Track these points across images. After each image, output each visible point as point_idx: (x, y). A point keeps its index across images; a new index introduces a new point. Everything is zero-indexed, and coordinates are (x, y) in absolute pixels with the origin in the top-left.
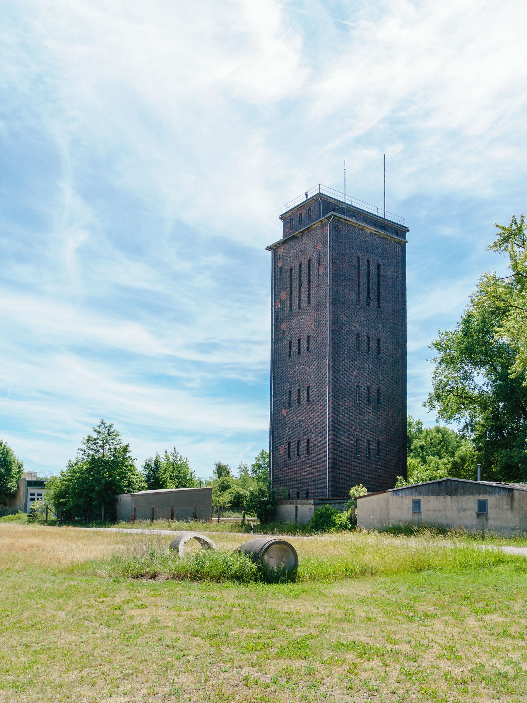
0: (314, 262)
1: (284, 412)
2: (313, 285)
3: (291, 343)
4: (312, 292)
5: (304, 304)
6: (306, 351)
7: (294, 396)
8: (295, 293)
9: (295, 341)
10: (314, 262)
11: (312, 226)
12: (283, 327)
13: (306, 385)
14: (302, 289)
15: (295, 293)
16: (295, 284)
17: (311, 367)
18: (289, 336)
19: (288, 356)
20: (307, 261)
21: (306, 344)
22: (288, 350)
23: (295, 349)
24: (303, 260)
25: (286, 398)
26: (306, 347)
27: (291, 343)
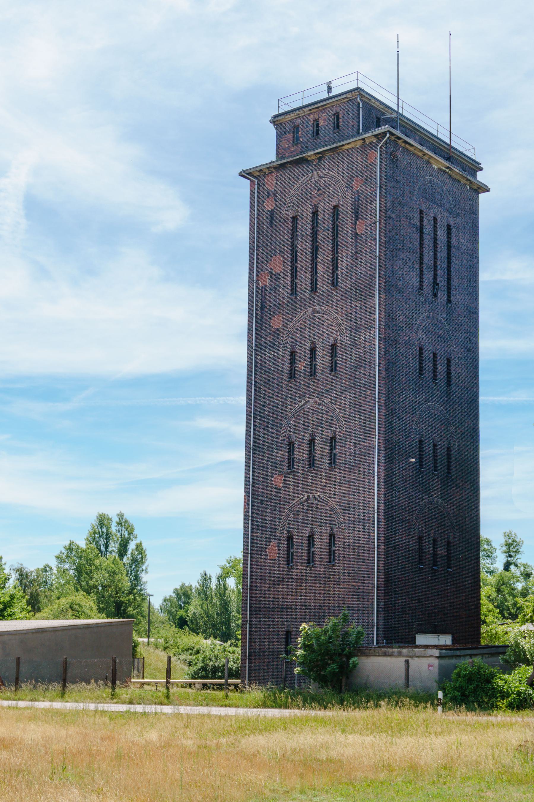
0: (346, 210)
1: (278, 481)
2: (344, 253)
3: (293, 354)
4: (342, 265)
5: (324, 285)
6: (327, 371)
7: (301, 453)
8: (304, 262)
9: (303, 351)
10: (346, 210)
11: (343, 145)
12: (277, 322)
13: (327, 434)
14: (320, 257)
15: (304, 262)
16: (304, 246)
17: (338, 402)
18: (290, 340)
19: (286, 377)
20: (331, 207)
21: (328, 358)
22: (287, 366)
23: (301, 365)
24: (322, 204)
25: (283, 454)
26: (327, 364)
27: (293, 354)
